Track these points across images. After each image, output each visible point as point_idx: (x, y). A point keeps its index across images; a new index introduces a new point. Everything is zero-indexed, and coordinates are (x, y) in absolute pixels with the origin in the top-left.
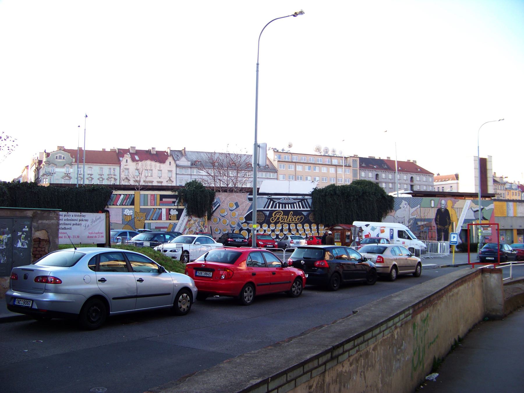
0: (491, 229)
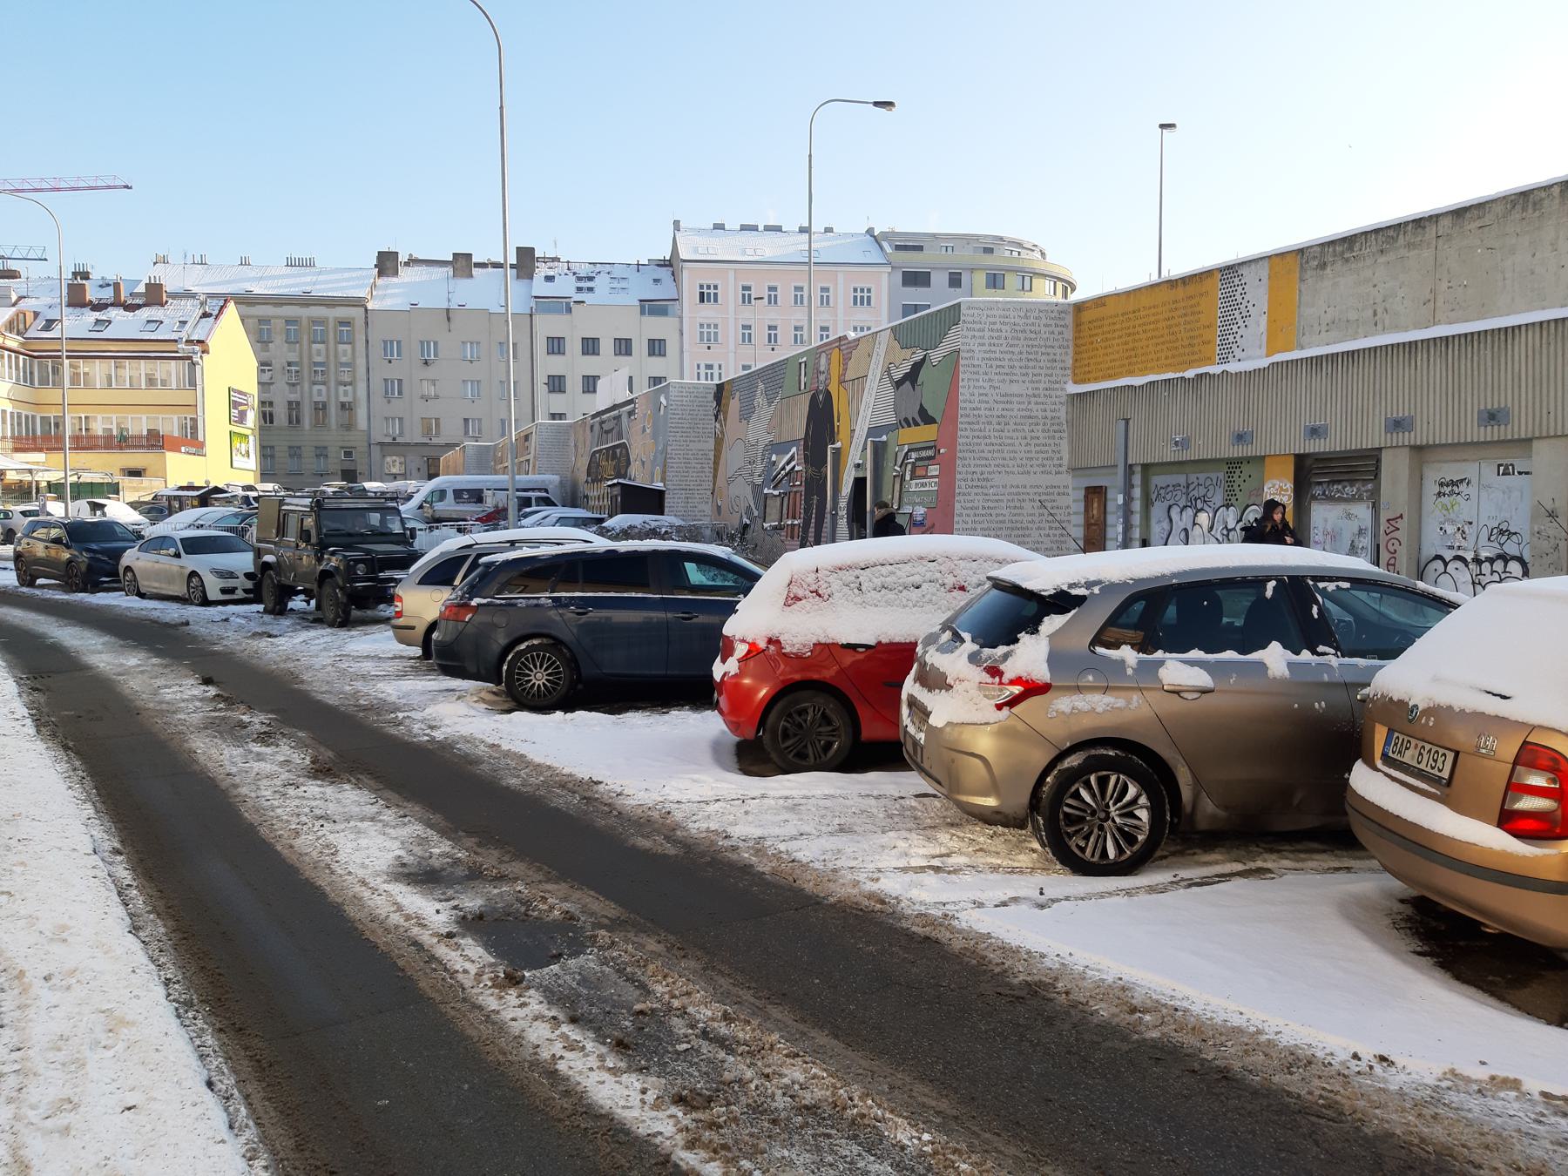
0: (937, 473)
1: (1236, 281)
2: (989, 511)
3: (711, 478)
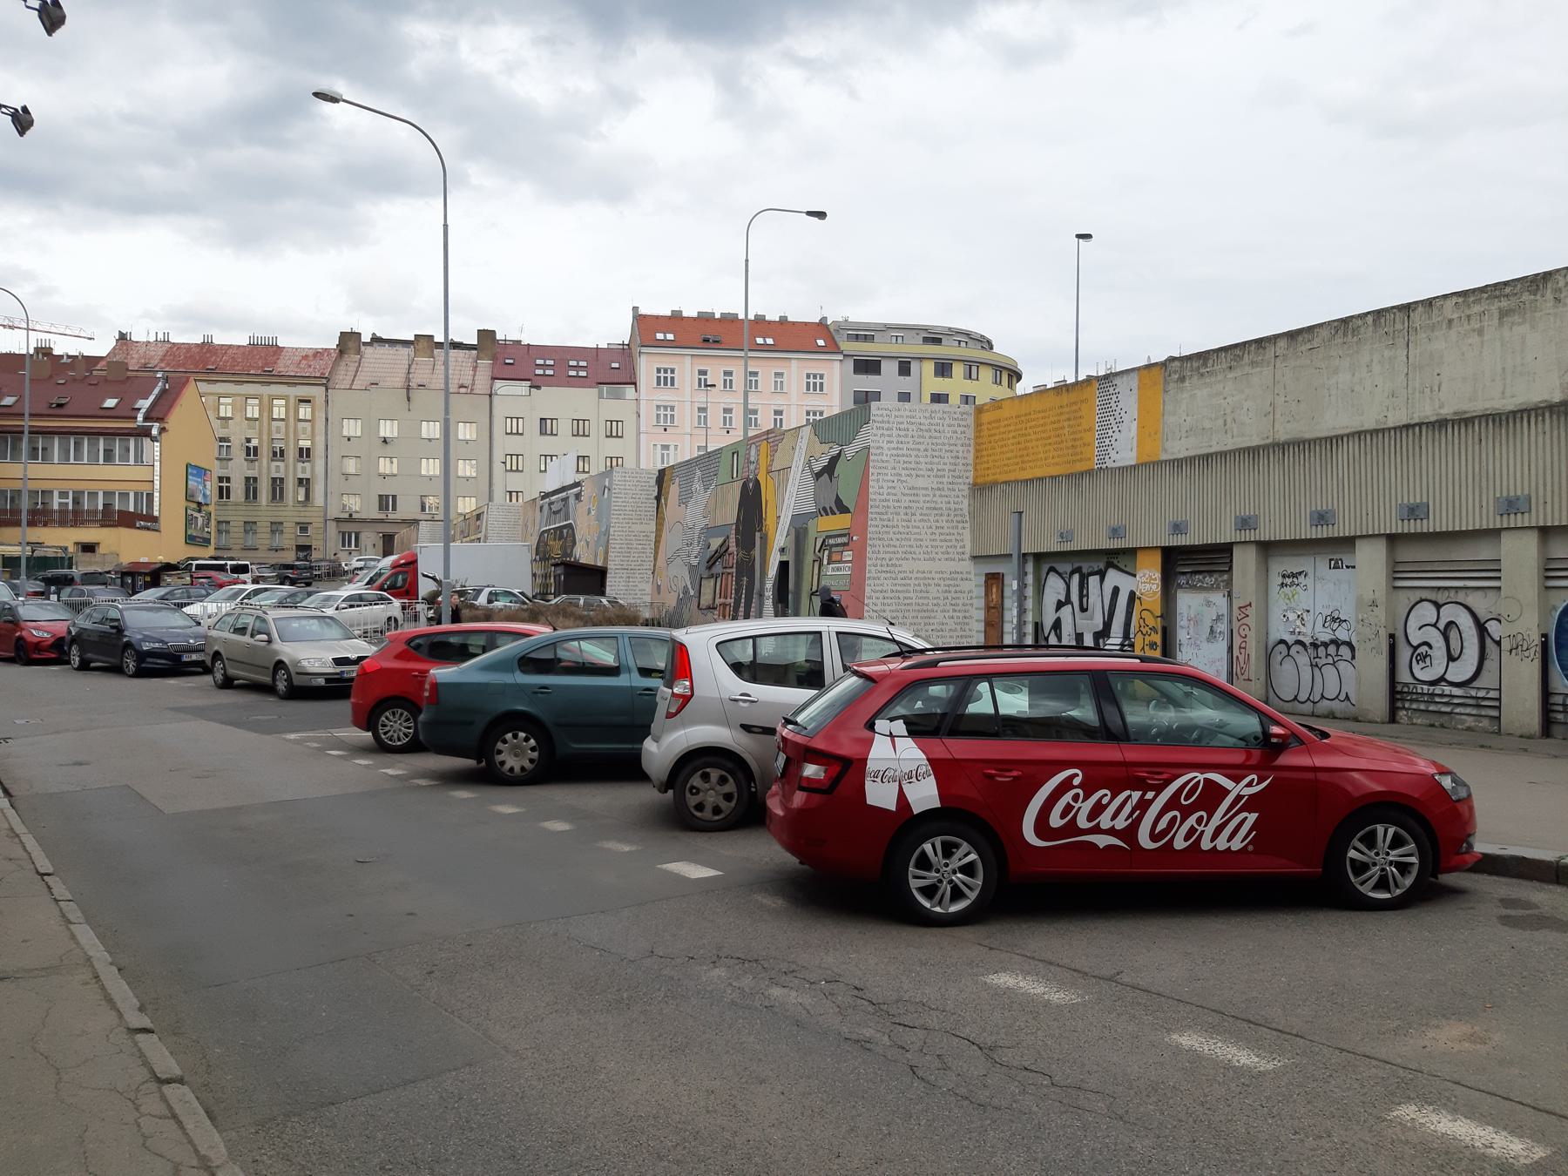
0: (850, 559)
1: (1111, 391)
2: (897, 595)
3: (652, 559)
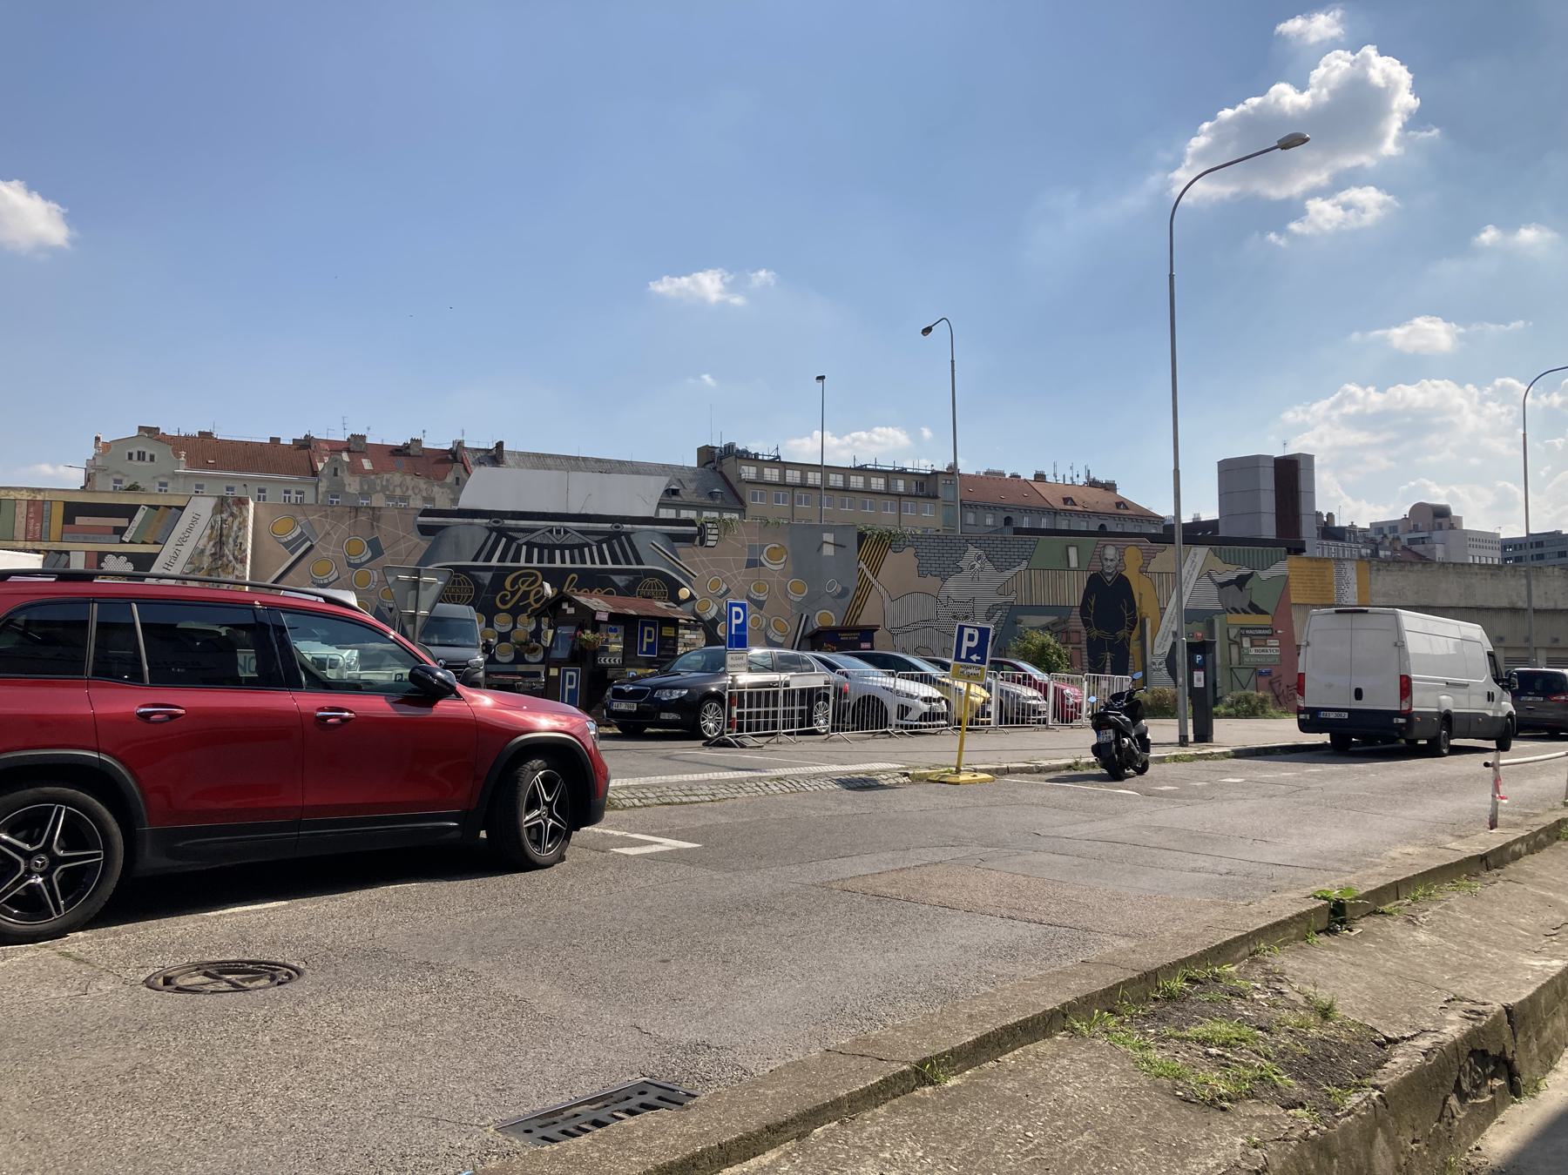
0: (1278, 644)
